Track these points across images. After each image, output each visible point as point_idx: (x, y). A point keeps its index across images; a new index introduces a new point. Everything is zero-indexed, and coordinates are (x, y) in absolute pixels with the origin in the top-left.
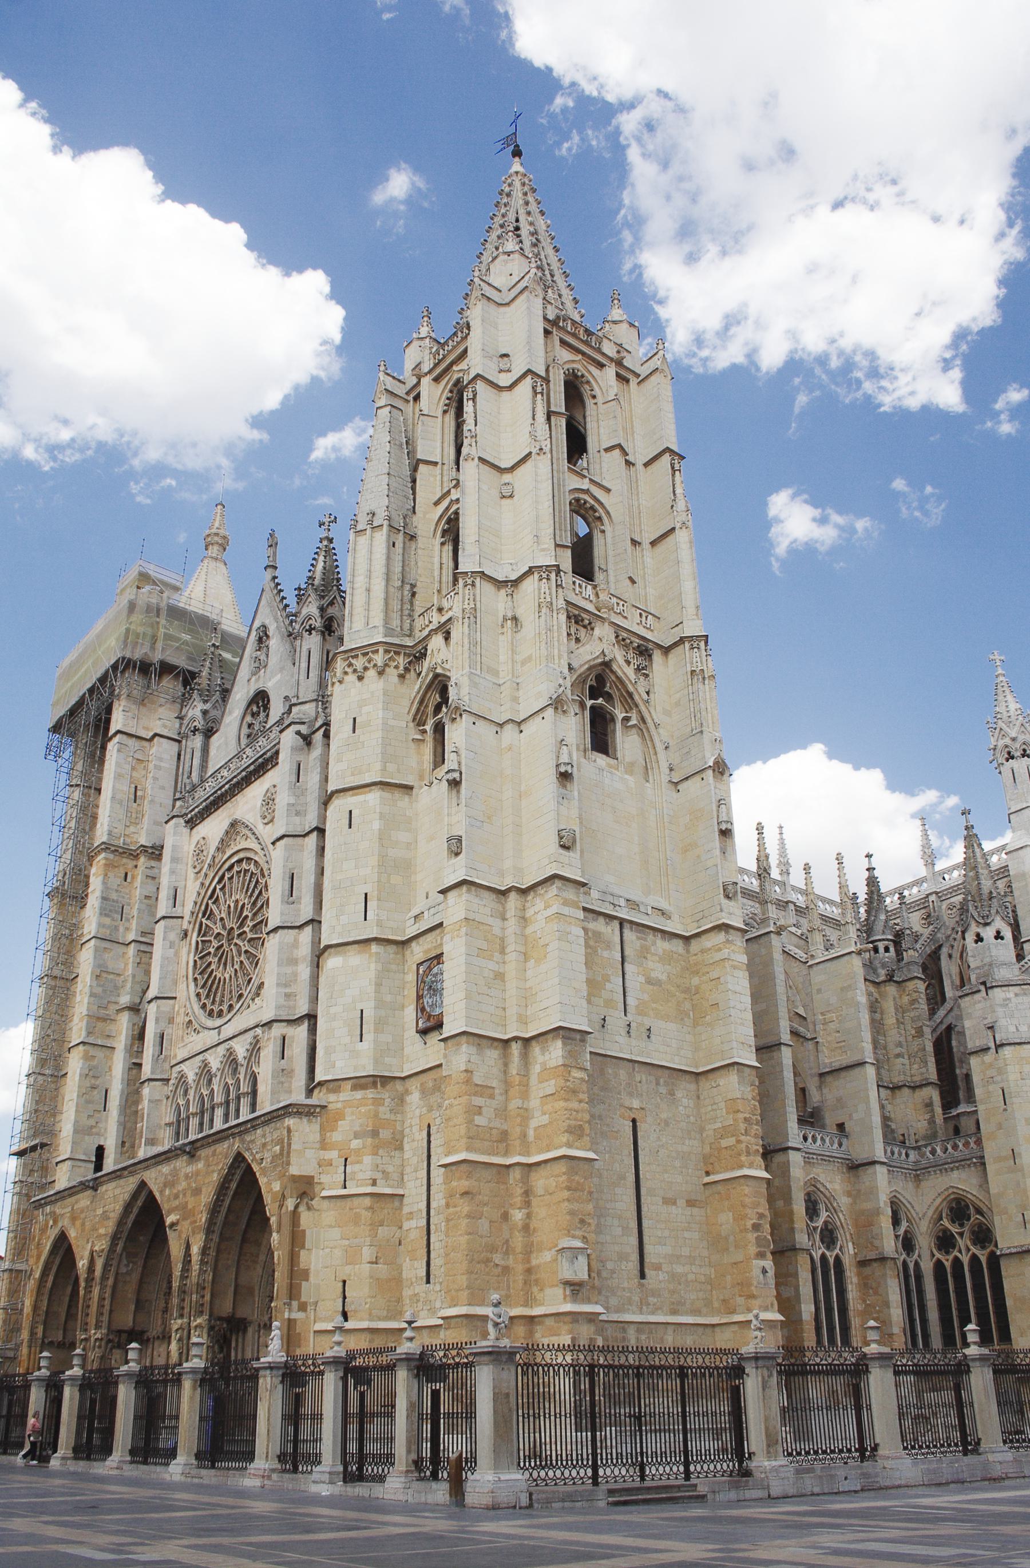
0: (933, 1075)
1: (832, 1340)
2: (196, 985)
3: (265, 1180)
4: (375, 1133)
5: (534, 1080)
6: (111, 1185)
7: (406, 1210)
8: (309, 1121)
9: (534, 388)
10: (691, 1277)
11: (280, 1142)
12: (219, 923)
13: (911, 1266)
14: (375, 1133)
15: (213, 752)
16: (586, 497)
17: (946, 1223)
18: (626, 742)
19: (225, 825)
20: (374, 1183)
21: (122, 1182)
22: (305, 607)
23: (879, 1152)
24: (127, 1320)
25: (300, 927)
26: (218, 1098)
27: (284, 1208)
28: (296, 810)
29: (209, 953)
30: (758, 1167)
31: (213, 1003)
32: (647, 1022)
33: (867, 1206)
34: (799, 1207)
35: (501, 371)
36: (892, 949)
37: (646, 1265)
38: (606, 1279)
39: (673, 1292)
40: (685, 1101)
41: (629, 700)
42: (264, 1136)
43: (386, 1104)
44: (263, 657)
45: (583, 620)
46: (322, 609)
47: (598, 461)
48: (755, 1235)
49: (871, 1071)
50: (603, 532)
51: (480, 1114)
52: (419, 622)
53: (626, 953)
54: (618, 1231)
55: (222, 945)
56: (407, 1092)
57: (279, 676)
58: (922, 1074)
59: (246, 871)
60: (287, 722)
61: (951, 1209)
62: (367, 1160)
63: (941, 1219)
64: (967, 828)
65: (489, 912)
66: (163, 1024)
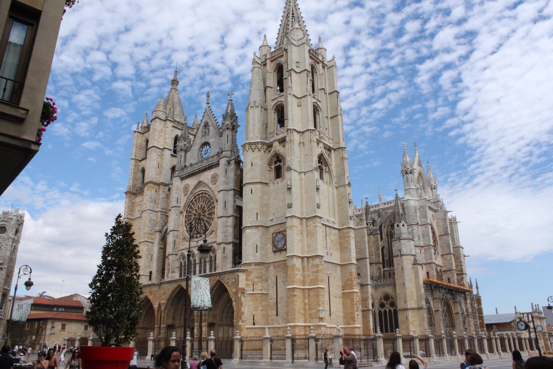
0: (381, 261)
2: (186, 228)
3: (229, 288)
5: (310, 267)
6: (166, 285)
7: (269, 297)
9: (307, 75)
11: (235, 278)
12: (194, 211)
14: (261, 277)
15: (188, 157)
16: (315, 104)
17: (383, 300)
18: (325, 176)
19: (196, 182)
20: (261, 290)
21: (171, 284)
24: (170, 322)
25: (228, 217)
26: (197, 261)
27: (237, 296)
28: (227, 183)
29: (191, 219)
32: (331, 251)
35: (297, 67)
36: (372, 225)
41: (326, 164)
42: (228, 276)
46: (232, 123)
49: (368, 260)
50: (319, 114)
52: (269, 136)
53: (327, 233)
56: (269, 267)
57: (214, 139)
61: (384, 297)
62: (260, 284)
63: (381, 299)
64: (397, 195)
66: (175, 238)
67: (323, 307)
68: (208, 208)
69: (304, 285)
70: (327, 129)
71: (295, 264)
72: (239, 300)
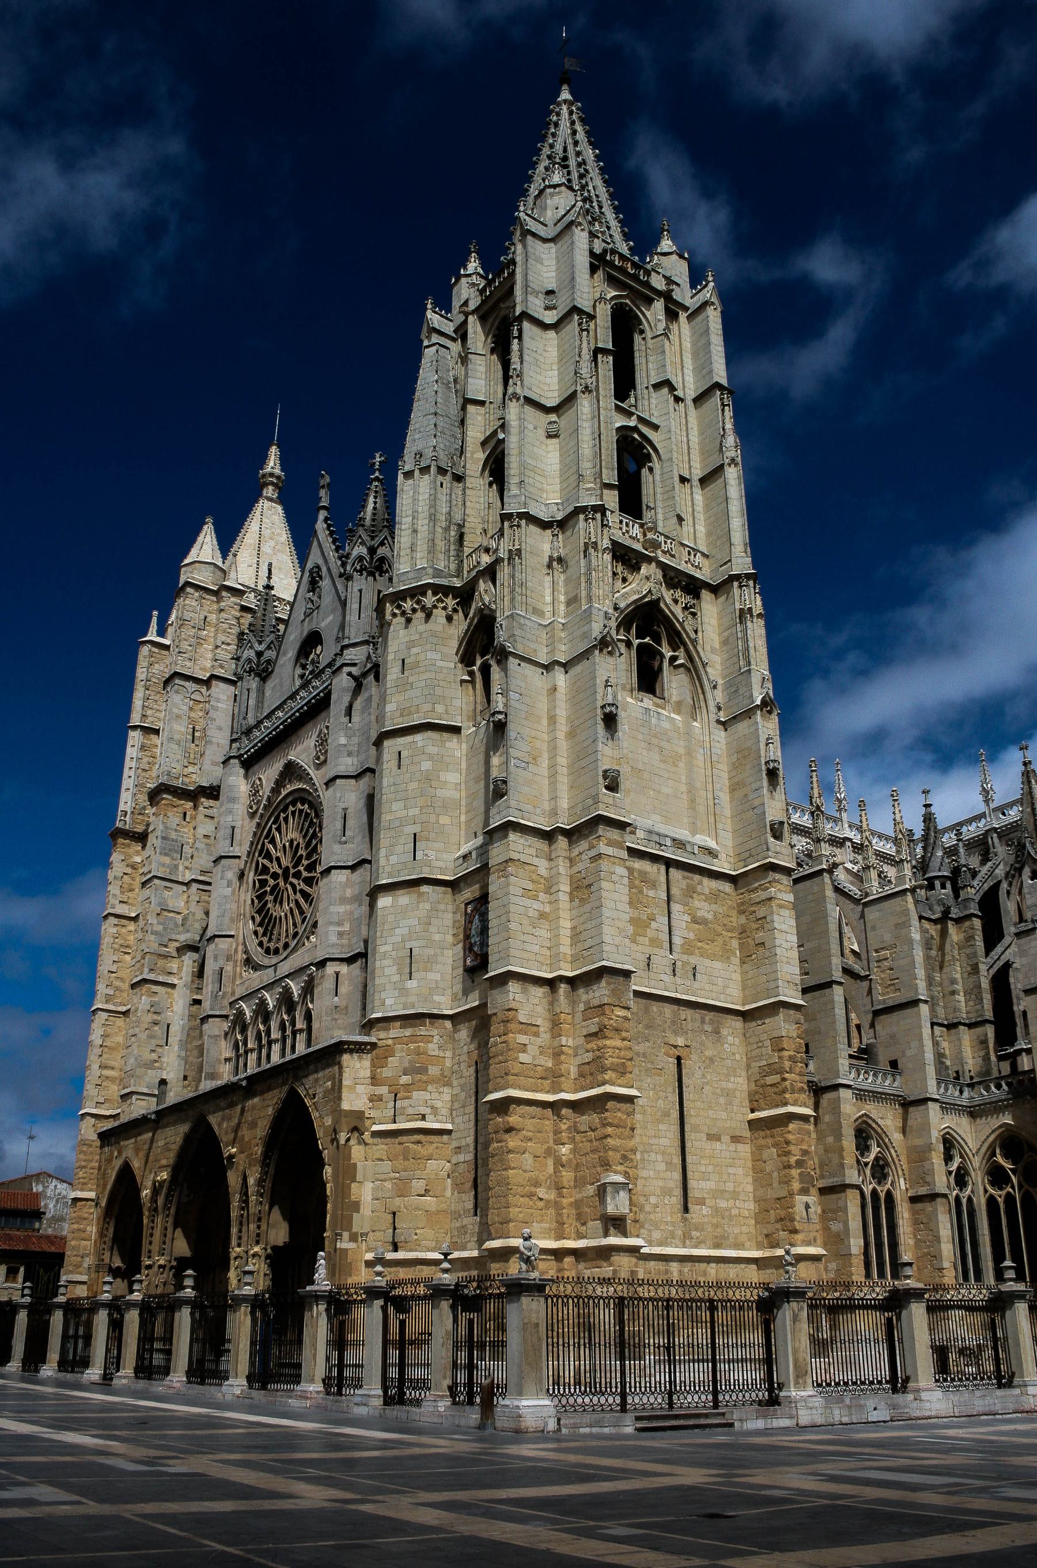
1: (882, 1275)
4: (423, 1070)
8: (360, 1058)
9: (580, 324)
10: (735, 1212)
12: (275, 863)
13: (964, 1201)
18: (674, 683)
22: (356, 548)
23: (932, 1089)
29: (266, 891)
30: (805, 1105)
31: (270, 940)
32: (693, 960)
33: (919, 1142)
34: (849, 1143)
37: (689, 1199)
38: (649, 1213)
39: (716, 1226)
40: (730, 1039)
41: (676, 640)
43: (435, 1041)
44: (315, 598)
45: (629, 560)
47: (646, 397)
48: (799, 1171)
50: (651, 470)
51: (524, 1052)
53: (674, 891)
54: (662, 1167)
55: (278, 884)
58: (977, 1011)
59: (301, 811)
60: (338, 664)
63: (994, 1154)
64: (1025, 764)
65: (533, 851)
67: (626, 1174)
68: (306, 848)
69: (555, 1089)
70: (680, 519)
71: (513, 1005)
72: (343, 1152)
